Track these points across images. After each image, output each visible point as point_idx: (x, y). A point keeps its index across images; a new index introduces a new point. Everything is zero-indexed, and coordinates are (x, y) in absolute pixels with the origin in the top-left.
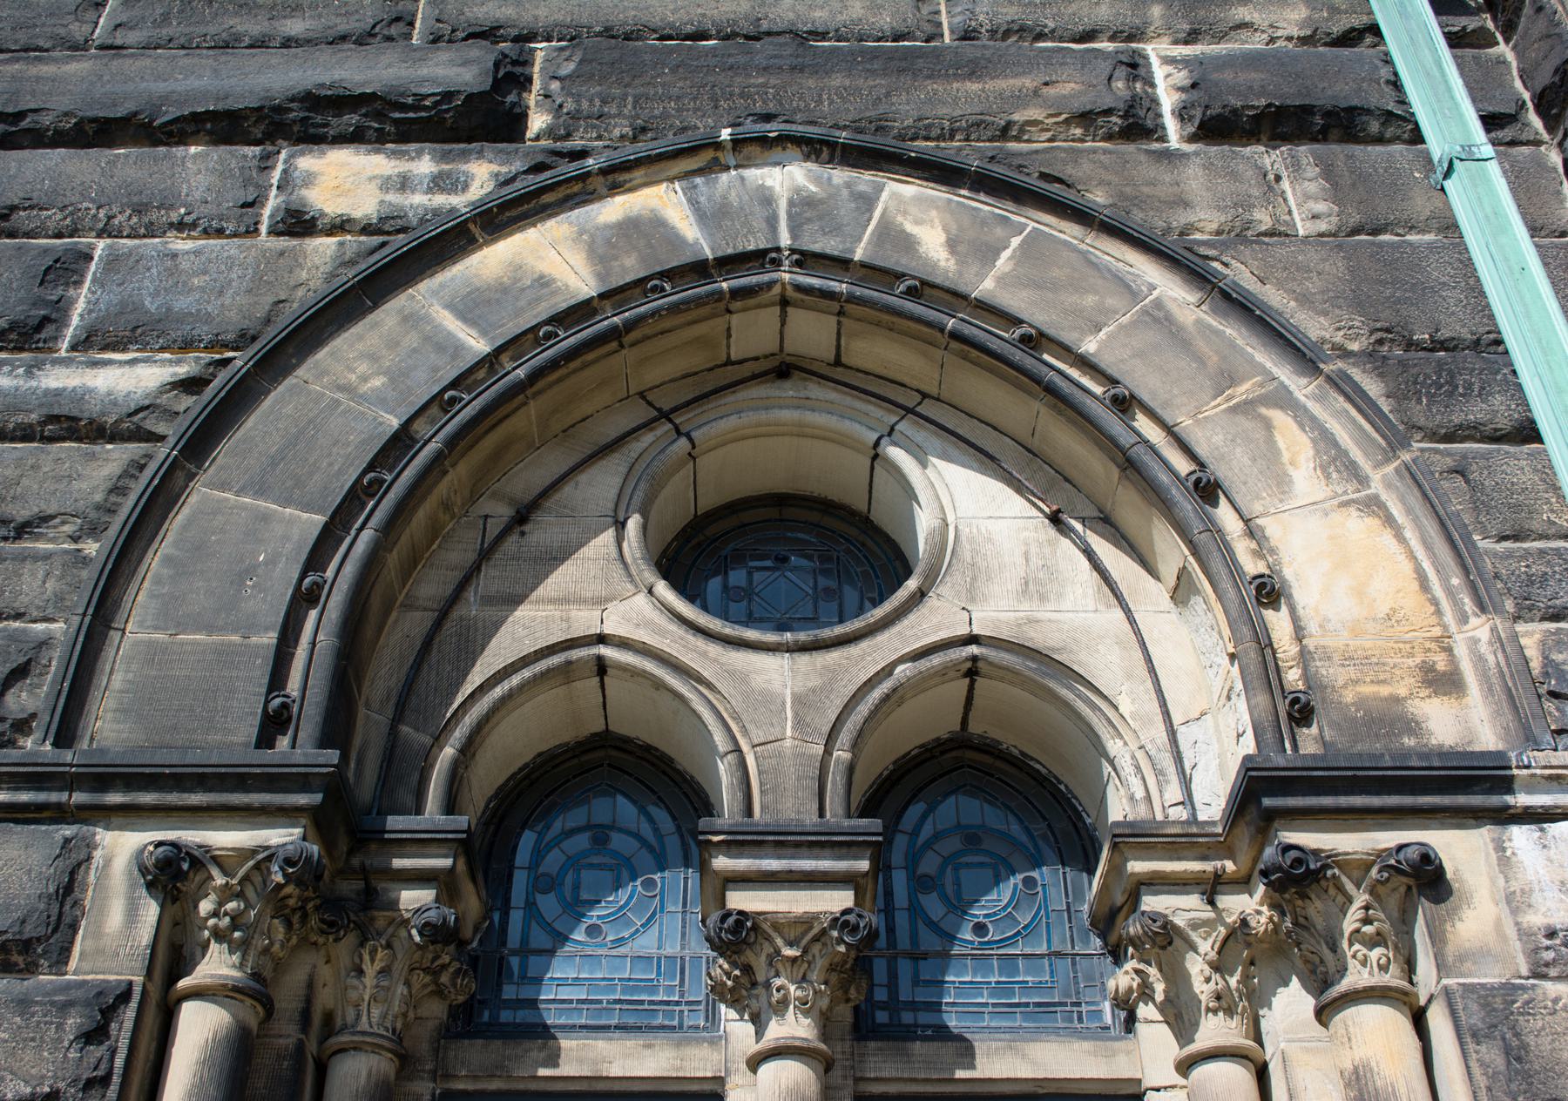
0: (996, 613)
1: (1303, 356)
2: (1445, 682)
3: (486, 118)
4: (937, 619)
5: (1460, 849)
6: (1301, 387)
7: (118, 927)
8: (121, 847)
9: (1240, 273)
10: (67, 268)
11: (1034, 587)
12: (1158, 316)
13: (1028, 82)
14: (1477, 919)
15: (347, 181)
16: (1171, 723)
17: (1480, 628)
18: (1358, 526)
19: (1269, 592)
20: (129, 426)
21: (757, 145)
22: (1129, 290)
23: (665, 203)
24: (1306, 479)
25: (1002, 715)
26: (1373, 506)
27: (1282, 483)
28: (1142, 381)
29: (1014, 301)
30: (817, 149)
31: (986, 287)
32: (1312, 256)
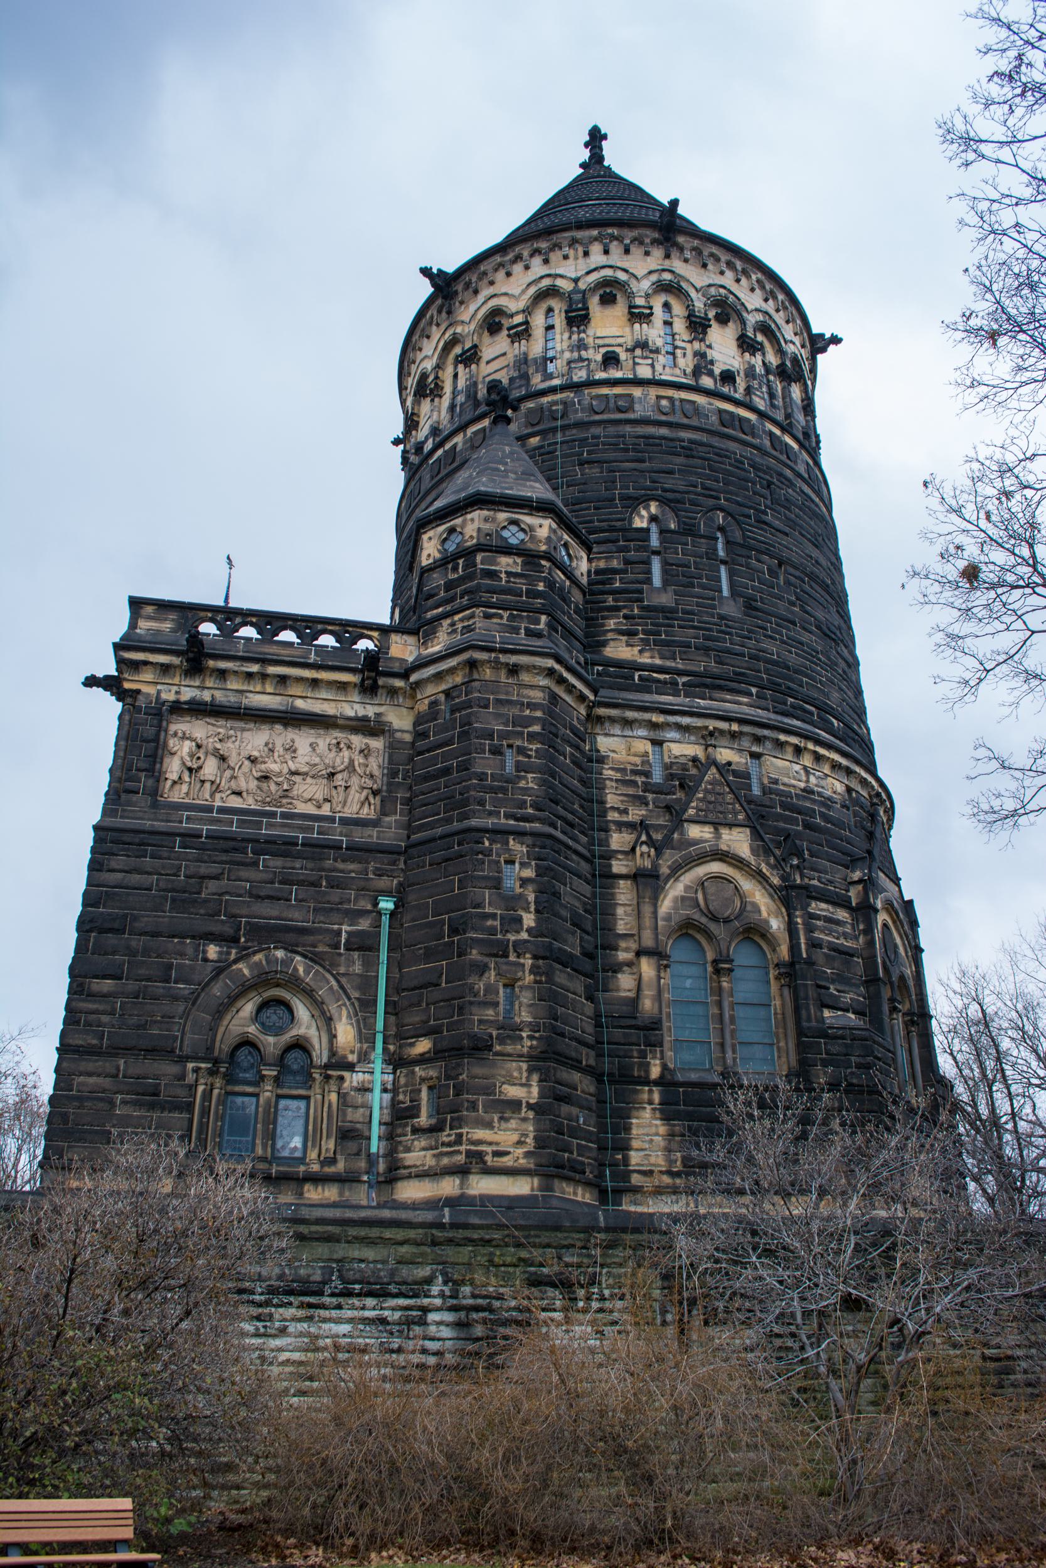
0: (302, 1031)
1: (349, 999)
2: (352, 1052)
3: (235, 940)
4: (294, 1032)
5: (347, 1074)
6: (348, 1003)
7: (191, 1077)
8: (190, 1065)
9: (343, 980)
10: (170, 967)
12: (331, 988)
13: (321, 937)
14: (346, 1084)
16: (320, 1055)
18: (349, 1027)
19: (335, 1036)
20: (186, 999)
22: (328, 982)
24: (344, 1019)
25: (302, 1042)
26: (352, 1024)
27: (341, 1019)
29: (311, 983)
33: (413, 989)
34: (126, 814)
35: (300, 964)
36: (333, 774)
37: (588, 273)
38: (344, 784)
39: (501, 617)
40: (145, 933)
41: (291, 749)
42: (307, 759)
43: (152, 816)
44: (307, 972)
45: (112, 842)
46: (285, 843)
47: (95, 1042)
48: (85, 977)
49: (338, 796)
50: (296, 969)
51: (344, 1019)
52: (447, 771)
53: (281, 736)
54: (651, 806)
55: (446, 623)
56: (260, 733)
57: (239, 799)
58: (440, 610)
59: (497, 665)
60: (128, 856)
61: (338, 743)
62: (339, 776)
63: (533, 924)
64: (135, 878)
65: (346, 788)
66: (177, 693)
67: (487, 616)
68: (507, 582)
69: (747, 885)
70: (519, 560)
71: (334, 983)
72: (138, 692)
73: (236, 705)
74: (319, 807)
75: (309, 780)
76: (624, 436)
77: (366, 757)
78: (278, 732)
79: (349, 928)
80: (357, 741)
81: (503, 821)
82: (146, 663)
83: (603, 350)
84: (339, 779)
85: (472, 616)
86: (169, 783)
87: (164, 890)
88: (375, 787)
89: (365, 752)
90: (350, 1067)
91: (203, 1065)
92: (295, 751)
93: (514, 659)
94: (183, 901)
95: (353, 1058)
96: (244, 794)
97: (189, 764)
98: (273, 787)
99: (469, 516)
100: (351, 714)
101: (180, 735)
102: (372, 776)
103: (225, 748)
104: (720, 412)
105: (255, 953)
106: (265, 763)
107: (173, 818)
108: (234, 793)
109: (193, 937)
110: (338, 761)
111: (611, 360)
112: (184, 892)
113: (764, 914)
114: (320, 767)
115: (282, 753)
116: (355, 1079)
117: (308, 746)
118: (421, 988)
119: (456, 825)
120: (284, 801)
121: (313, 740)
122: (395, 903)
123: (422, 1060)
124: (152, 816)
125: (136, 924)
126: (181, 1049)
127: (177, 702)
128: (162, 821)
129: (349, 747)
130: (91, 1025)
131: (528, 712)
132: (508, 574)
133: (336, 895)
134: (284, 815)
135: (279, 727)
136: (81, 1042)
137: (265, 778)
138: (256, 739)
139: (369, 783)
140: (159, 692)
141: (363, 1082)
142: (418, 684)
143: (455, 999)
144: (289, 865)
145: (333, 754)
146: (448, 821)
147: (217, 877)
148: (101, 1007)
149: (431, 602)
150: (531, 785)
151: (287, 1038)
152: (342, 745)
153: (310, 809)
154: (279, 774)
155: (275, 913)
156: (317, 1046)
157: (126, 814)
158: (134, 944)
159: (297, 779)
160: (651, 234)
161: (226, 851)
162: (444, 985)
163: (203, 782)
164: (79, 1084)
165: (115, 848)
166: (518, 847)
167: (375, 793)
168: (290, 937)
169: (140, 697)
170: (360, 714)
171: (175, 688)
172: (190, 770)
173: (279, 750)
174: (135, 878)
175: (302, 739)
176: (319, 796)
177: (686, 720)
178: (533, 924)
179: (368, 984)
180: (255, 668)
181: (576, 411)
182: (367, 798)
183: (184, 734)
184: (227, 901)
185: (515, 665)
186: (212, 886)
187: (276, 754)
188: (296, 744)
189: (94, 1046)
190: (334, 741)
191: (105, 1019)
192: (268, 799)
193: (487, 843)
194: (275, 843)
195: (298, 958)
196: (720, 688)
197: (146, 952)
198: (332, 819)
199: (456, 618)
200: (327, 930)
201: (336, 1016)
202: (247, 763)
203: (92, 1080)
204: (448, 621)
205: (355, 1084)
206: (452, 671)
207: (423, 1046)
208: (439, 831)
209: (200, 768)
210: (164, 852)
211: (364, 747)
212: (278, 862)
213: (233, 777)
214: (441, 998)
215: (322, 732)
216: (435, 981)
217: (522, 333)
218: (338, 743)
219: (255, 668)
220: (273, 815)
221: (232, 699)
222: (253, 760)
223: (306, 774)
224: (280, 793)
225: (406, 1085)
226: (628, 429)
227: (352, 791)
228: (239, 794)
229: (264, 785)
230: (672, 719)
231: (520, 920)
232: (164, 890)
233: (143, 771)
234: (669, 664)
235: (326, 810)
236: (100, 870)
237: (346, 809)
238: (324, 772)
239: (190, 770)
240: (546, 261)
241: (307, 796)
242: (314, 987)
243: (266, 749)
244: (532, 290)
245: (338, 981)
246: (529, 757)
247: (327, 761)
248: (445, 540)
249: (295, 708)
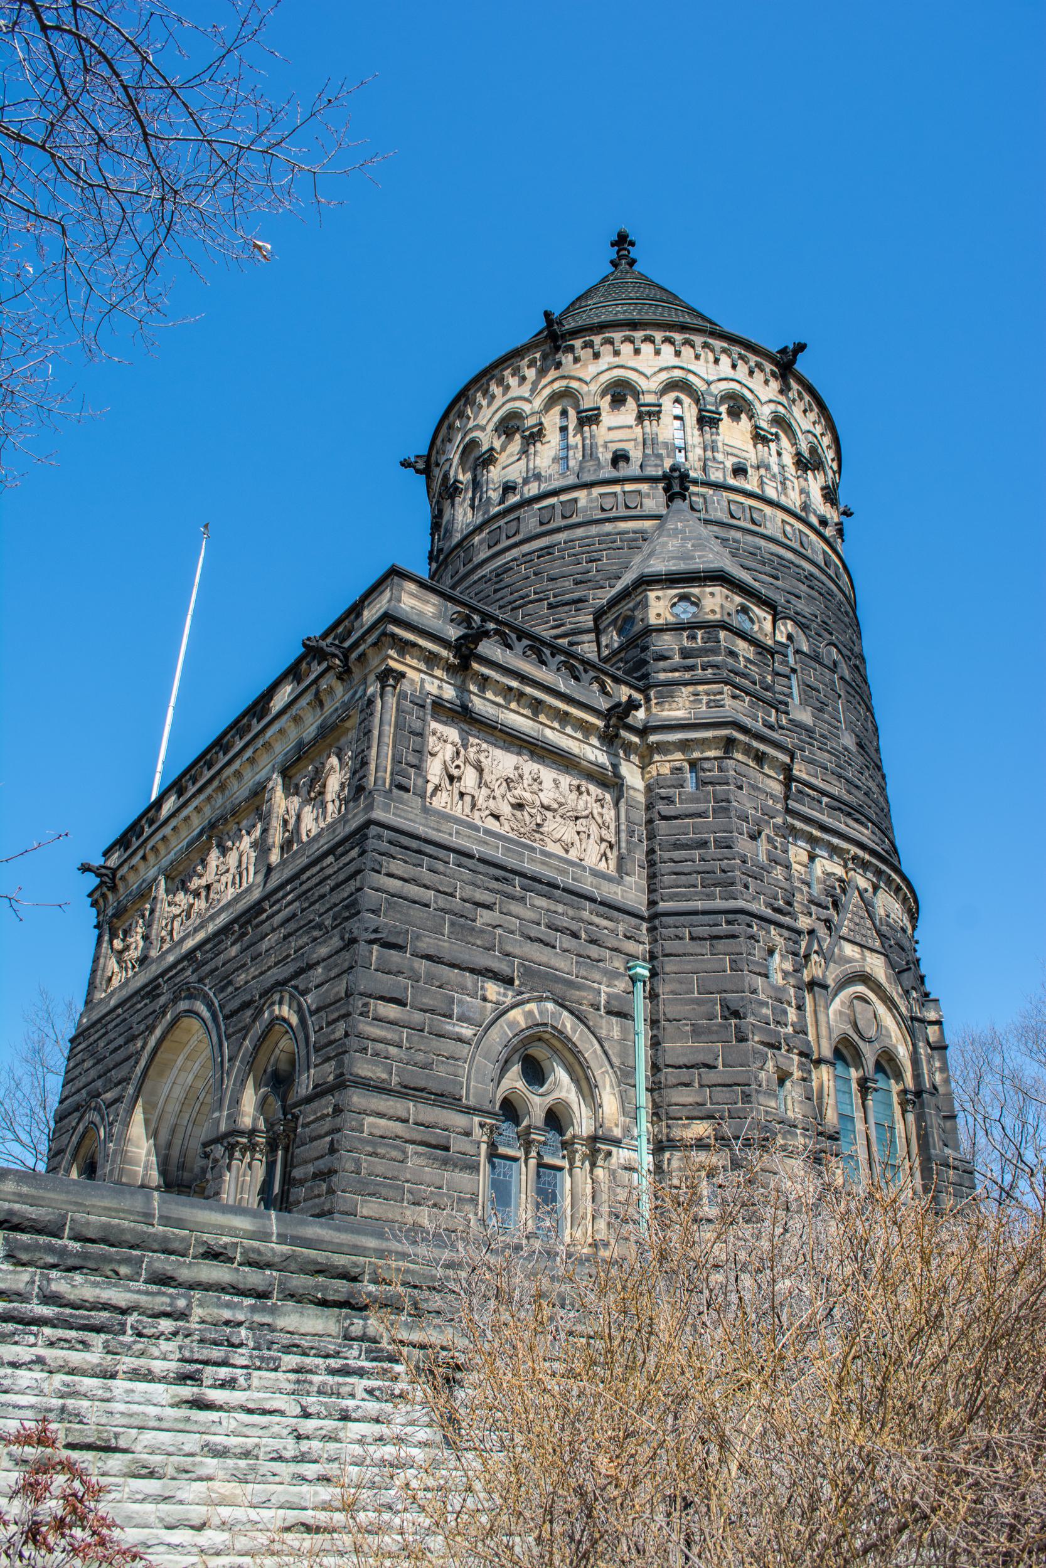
0: (563, 1095)
1: (612, 1067)
2: (617, 1125)
4: (555, 1095)
5: (614, 1150)
6: (610, 1071)
7: (477, 1131)
8: (476, 1119)
11: (568, 1091)
12: (595, 1052)
14: (614, 1160)
15: (492, 990)
16: (583, 1124)
17: (622, 1118)
18: (612, 1097)
21: (547, 999)
23: (532, 1006)
24: (608, 1086)
28: (592, 1065)
30: (556, 1002)
31: (574, 1039)
32: (616, 1044)
33: (680, 1067)
34: (398, 812)
35: (567, 1022)
36: (577, 818)
37: (720, 380)
39: (744, 701)
40: (428, 957)
43: (423, 821)
44: (574, 1031)
45: (390, 842)
46: (549, 884)
47: (384, 1076)
48: (370, 996)
50: (563, 1024)
51: (608, 1086)
52: (704, 844)
53: (531, 767)
54: (814, 916)
55: (686, 691)
58: (677, 674)
59: (748, 750)
60: (406, 862)
63: (795, 1020)
64: (413, 890)
67: (734, 697)
68: (746, 667)
69: (881, 1009)
70: (752, 649)
71: (597, 1046)
72: (403, 675)
75: (558, 819)
76: (760, 549)
79: (607, 989)
81: (763, 908)
82: (414, 645)
83: (736, 460)
85: (721, 693)
87: (442, 910)
90: (617, 1142)
91: (488, 1121)
92: (541, 783)
93: (762, 747)
94: (462, 926)
95: (617, 1132)
98: (527, 818)
99: (708, 590)
100: (592, 758)
101: (438, 735)
104: (824, 552)
105: (528, 1001)
107: (444, 827)
108: (492, 815)
109: (472, 971)
110: (581, 804)
111: (739, 471)
112: (462, 916)
113: (894, 1040)
115: (530, 781)
116: (621, 1155)
118: (692, 1067)
119: (719, 904)
121: (555, 776)
122: (650, 970)
123: (701, 1144)
124: (423, 821)
125: (419, 944)
126: (467, 1098)
128: (434, 829)
129: (588, 794)
130: (377, 1055)
131: (770, 802)
132: (747, 660)
133: (594, 951)
136: (370, 1074)
140: (423, 681)
141: (630, 1160)
142: (660, 748)
143: (739, 1085)
144: (553, 908)
145: (574, 795)
146: (711, 897)
147: (488, 907)
148: (389, 1036)
149: (662, 664)
150: (780, 877)
151: (549, 1100)
155: (544, 959)
156: (577, 1114)
157: (398, 812)
158: (416, 965)
159: (549, 814)
160: (769, 367)
161: (497, 879)
162: (721, 1068)
164: (371, 1125)
165: (393, 850)
166: (777, 938)
168: (559, 988)
169: (404, 681)
174: (413, 890)
175: (548, 774)
177: (835, 841)
178: (795, 1020)
179: (627, 1051)
180: (514, 684)
181: (716, 510)
184: (500, 935)
185: (764, 753)
186: (484, 917)
187: (525, 782)
188: (541, 775)
189: (384, 1080)
191: (393, 1050)
193: (755, 928)
194: (540, 882)
195: (565, 1013)
196: (849, 815)
197: (430, 978)
199: (700, 688)
200: (590, 987)
201: (600, 1084)
203: (383, 1122)
204: (690, 689)
205: (622, 1161)
206: (703, 743)
207: (701, 1129)
208: (699, 905)
210: (440, 866)
211: (601, 797)
212: (542, 902)
214: (720, 1081)
216: (710, 1062)
217: (648, 414)
219: (514, 684)
221: (491, 711)
225: (680, 1169)
226: (762, 543)
228: (497, 817)
229: (518, 813)
230: (826, 837)
231: (785, 1013)
232: (442, 910)
233: (412, 766)
234: (813, 780)
236: (379, 872)
240: (678, 354)
242: (581, 1048)
244: (664, 376)
245: (602, 1046)
246: (776, 848)
248: (674, 605)
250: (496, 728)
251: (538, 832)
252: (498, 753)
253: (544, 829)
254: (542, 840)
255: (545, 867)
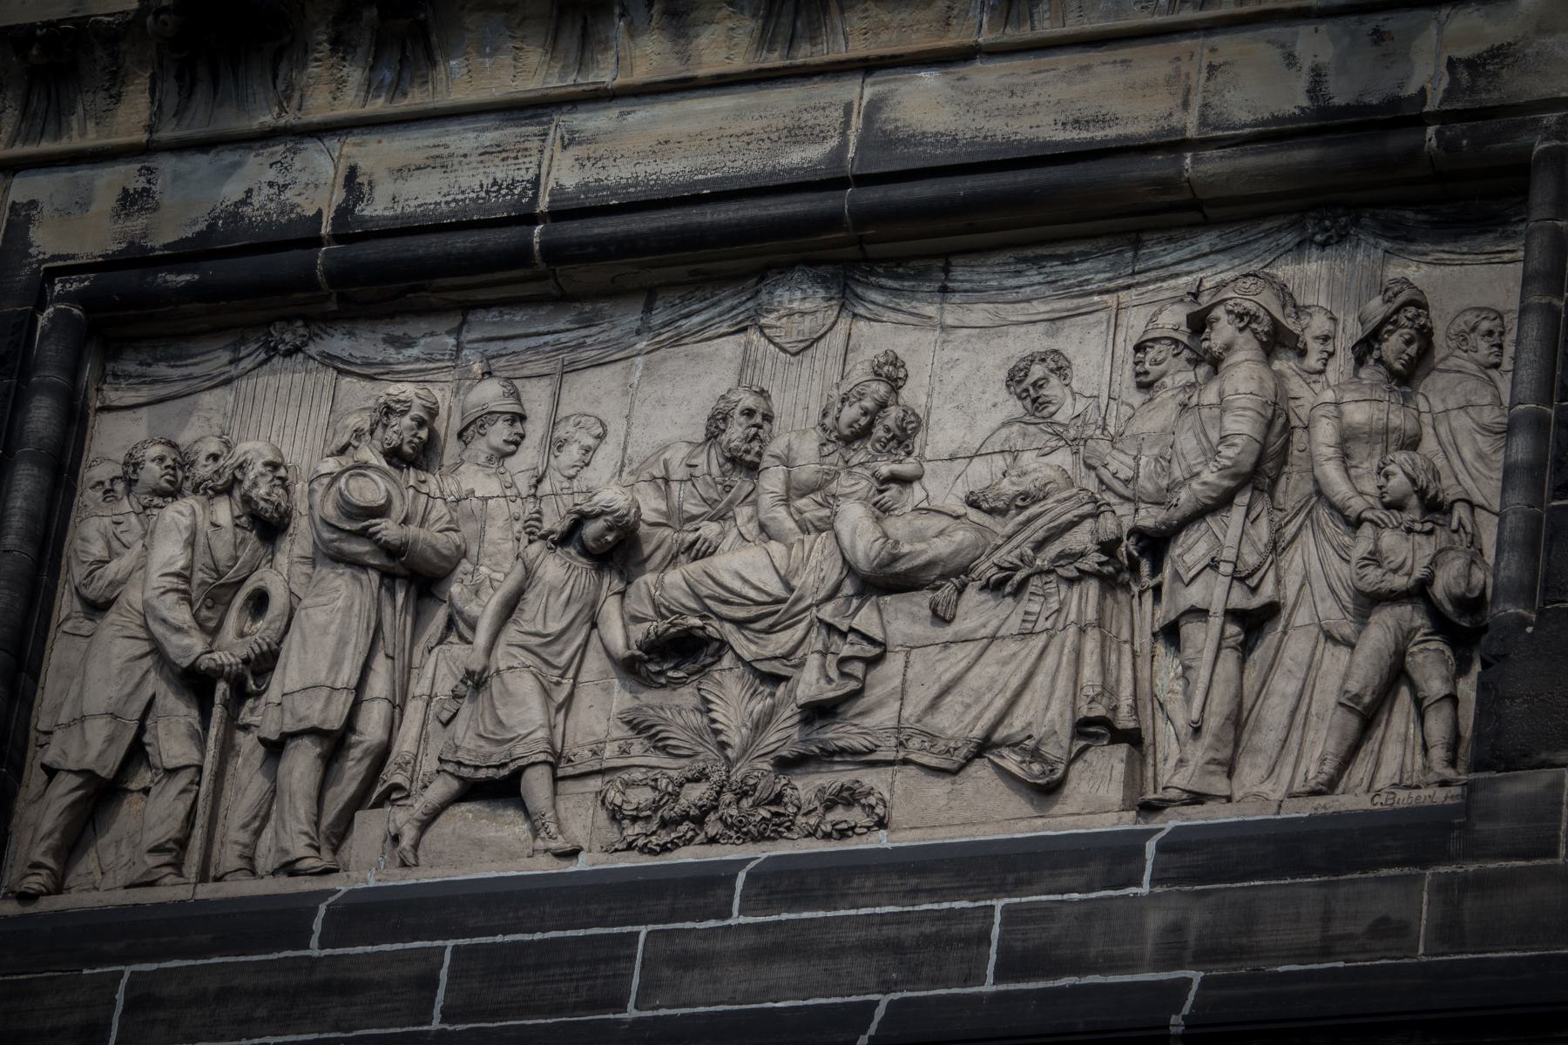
36: (1155, 544)
38: (1213, 593)
41: (878, 429)
42: (980, 474)
49: (1183, 690)
53: (800, 358)
56: (675, 360)
57: (507, 828)
61: (1199, 323)
62: (1191, 550)
65: (1254, 623)
66: (130, 201)
73: (499, 206)
74: (1047, 791)
75: (977, 612)
77: (1405, 378)
78: (792, 330)
80: (1323, 285)
84: (1199, 574)
86: (64, 792)
88: (1447, 581)
89: (1402, 354)
92: (902, 439)
96: (537, 784)
97: (188, 646)
101: (152, 473)
102: (1434, 507)
103: (420, 513)
106: (698, 551)
114: (1054, 510)
117: (985, 386)
120: (806, 786)
127: (135, 259)
129: (1277, 341)
134: (779, 883)
135: (798, 305)
137: (678, 651)
138: (635, 412)
139: (1407, 552)
152: (1223, 331)
153: (984, 812)
154: (771, 613)
159: (901, 619)
163: (275, 749)
167: (1461, 626)
170: (1340, 93)
171: (110, 180)
172: (196, 683)
173: (798, 440)
176: (1045, 715)
182: (1397, 674)
183: (182, 462)
188: (913, 394)
190: (1174, 318)
192: (695, 794)
198: (1112, 857)
202: (554, 568)
209: (264, 663)
213: (476, 682)
215: (1094, 271)
218: (1199, 323)
220: (707, 887)
222: (615, 550)
223: (958, 572)
224: (784, 734)
227: (1294, 645)
228: (498, 789)
229: (675, 706)
235: (1096, 799)
237: (1250, 775)
238: (1080, 539)
239: (196, 683)
241: (958, 722)
243: (710, 463)
247: (1120, 464)
249: (890, 141)
250: (518, 256)
251: (829, 756)
252: (595, 392)
253: (874, 722)
254: (848, 797)
255: (784, 972)
